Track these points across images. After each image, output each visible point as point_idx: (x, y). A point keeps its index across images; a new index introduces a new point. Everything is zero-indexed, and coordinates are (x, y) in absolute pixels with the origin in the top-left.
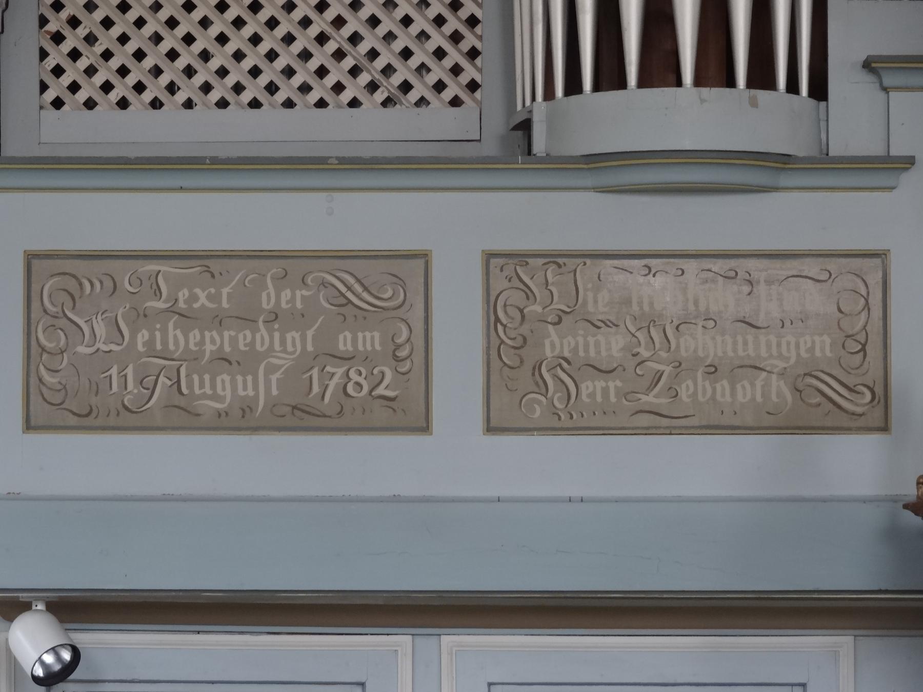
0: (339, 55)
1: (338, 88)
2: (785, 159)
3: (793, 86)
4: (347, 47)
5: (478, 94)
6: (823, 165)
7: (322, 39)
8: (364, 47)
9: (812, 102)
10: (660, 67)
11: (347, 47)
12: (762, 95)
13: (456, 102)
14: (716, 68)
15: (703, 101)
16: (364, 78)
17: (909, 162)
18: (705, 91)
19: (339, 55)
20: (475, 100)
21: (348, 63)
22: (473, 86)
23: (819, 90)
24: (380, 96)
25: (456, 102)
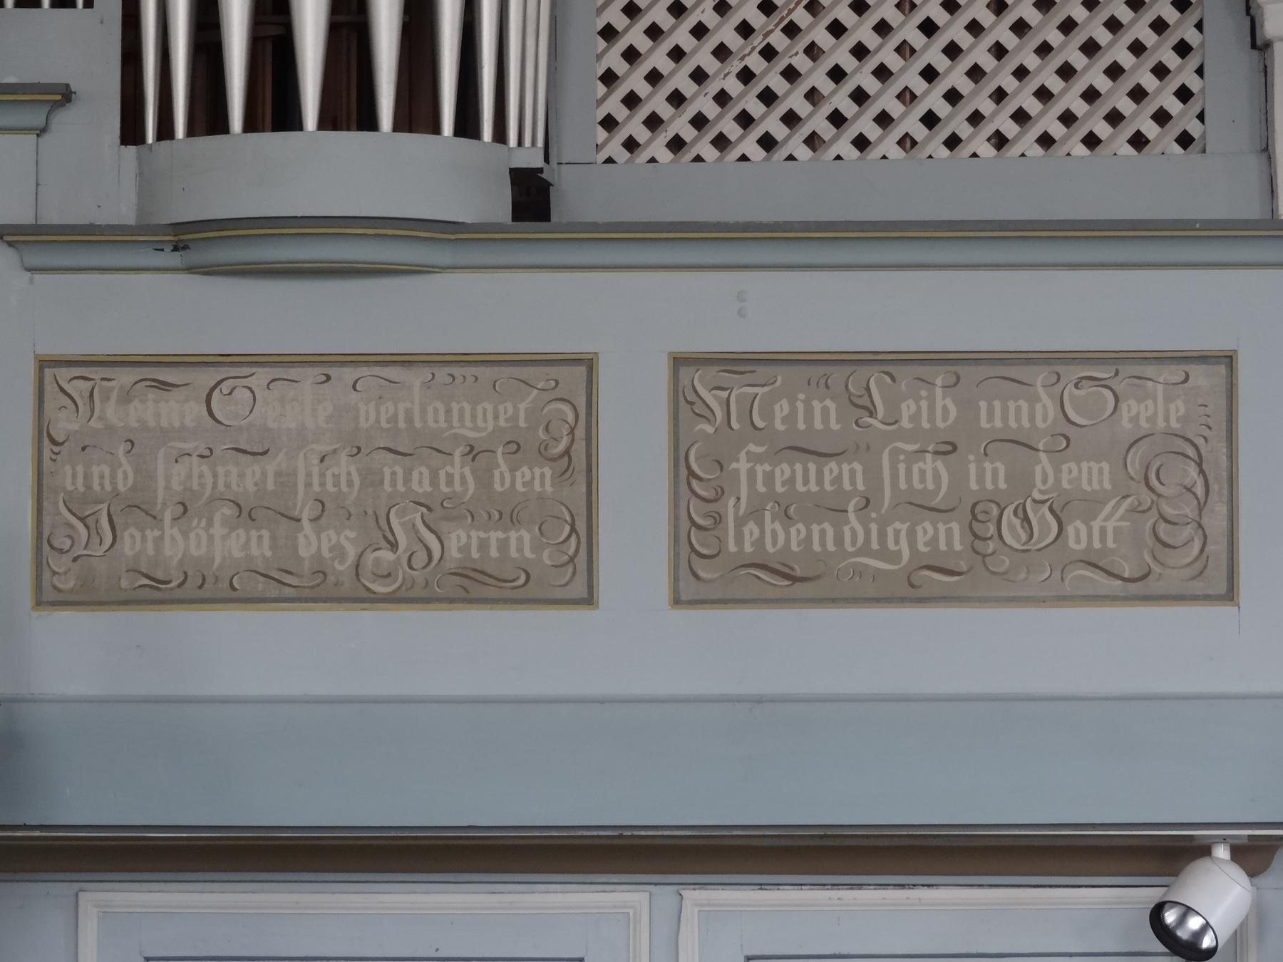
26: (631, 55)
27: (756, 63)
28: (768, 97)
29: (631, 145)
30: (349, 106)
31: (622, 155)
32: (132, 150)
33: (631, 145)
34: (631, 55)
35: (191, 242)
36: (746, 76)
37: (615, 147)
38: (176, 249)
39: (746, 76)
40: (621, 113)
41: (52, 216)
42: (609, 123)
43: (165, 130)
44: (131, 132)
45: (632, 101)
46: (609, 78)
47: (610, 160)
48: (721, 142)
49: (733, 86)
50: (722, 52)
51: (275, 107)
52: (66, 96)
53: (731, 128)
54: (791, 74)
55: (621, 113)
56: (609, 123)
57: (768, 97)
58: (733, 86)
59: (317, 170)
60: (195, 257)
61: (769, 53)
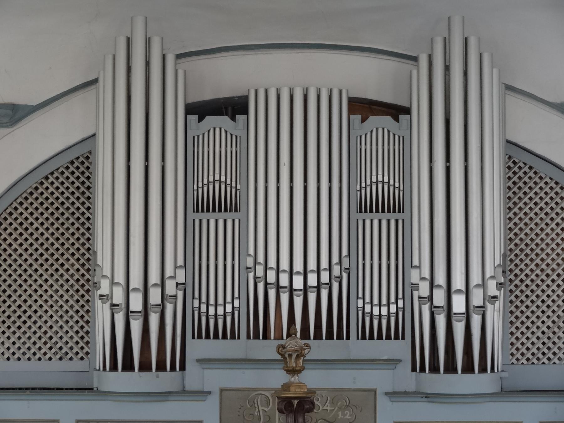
0: (45, 343)
1: (45, 354)
2: (170, 393)
3: (173, 368)
4: (48, 341)
5: (89, 356)
6: (183, 393)
7: (40, 338)
8: (53, 341)
9: (181, 372)
10: (128, 366)
11: (48, 341)
12: (161, 374)
13: (82, 359)
14: (145, 367)
15: (140, 377)
16: (53, 351)
17: (209, 393)
18: (141, 373)
19: (45, 343)
20: (88, 358)
21: (48, 345)
22: (87, 353)
23: (183, 368)
24: (58, 356)
25: (82, 359)
26: (517, 339)
27: (546, 340)
28: (549, 348)
29: (517, 360)
30: (468, 368)
31: (515, 362)
32: (414, 373)
33: (517, 360)
34: (517, 339)
35: (428, 397)
36: (544, 343)
37: (514, 361)
38: (426, 397)
39: (544, 343)
40: (515, 352)
41: (397, 390)
42: (512, 354)
43: (423, 369)
44: (414, 369)
45: (517, 349)
46: (512, 344)
47: (513, 364)
48: (538, 359)
49: (541, 346)
50: (538, 338)
51: (451, 368)
52: (400, 361)
53: (540, 356)
54: (554, 343)
55: (515, 352)
56: (512, 354)
57: (549, 348)
58: (541, 346)
59: (461, 383)
60: (429, 399)
61: (549, 338)
